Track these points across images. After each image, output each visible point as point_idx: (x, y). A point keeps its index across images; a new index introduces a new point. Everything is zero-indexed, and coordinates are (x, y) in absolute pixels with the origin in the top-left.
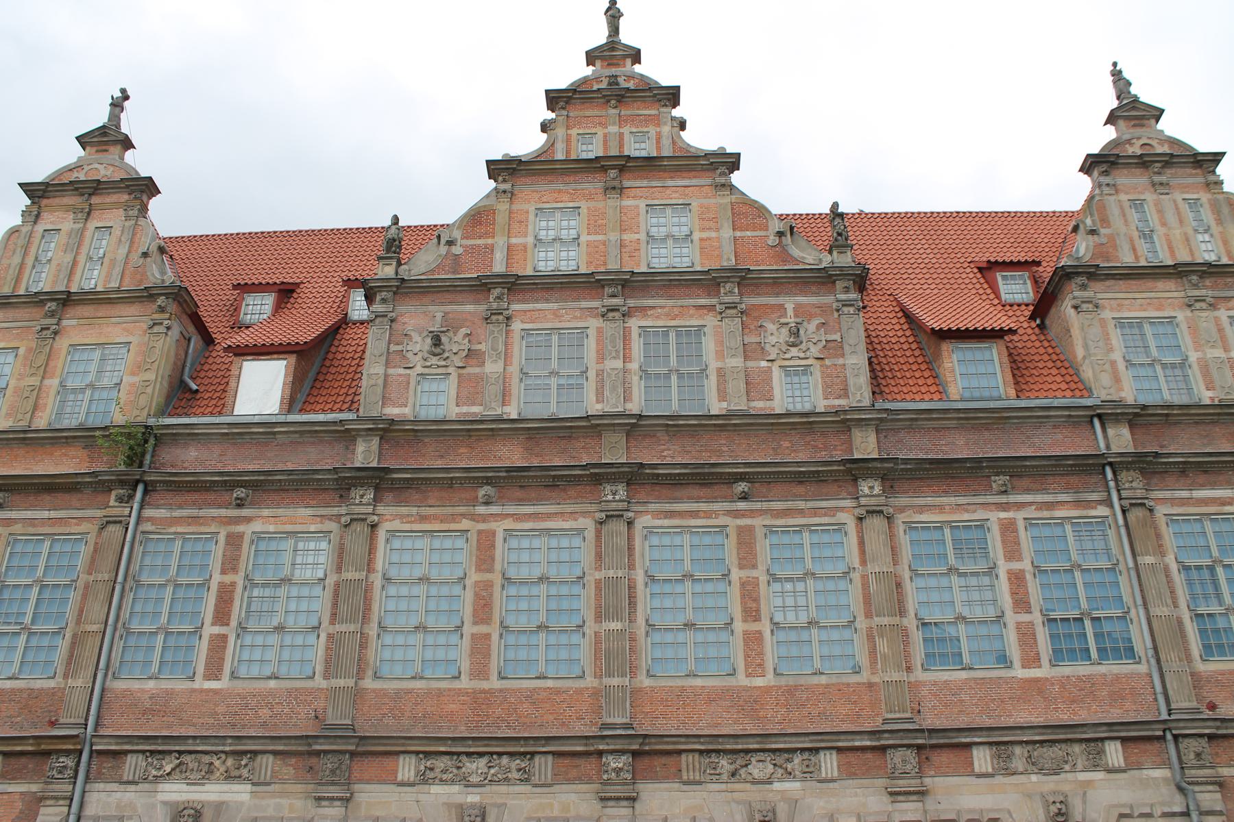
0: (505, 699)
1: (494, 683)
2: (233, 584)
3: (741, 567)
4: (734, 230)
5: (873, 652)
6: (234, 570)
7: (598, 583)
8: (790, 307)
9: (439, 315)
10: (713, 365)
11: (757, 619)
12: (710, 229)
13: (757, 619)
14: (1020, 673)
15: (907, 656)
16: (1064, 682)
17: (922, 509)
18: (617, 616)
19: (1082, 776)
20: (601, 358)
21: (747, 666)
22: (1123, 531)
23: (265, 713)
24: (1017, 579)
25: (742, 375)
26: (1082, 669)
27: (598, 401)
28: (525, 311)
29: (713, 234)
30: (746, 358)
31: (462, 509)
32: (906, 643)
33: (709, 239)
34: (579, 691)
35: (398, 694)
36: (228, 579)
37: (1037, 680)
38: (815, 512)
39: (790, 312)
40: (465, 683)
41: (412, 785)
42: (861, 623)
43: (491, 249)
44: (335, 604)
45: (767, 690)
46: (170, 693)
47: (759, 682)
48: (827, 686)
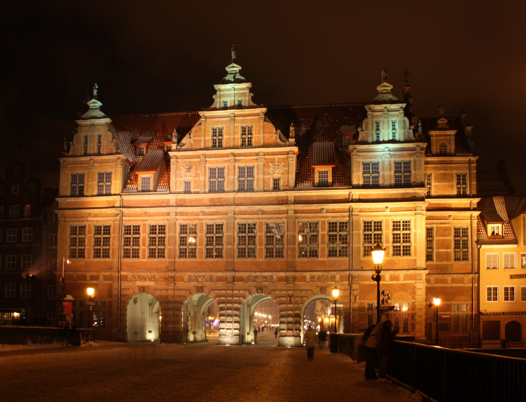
0: (206, 264)
1: (204, 260)
2: (145, 236)
3: (259, 232)
4: (264, 133)
5: (287, 253)
6: (145, 232)
7: (227, 236)
8: (276, 159)
9: (188, 163)
10: (256, 177)
11: (262, 245)
12: (257, 133)
13: (262, 245)
14: (320, 259)
15: (295, 255)
16: (330, 262)
17: (303, 218)
18: (231, 244)
19: (330, 283)
20: (228, 175)
21: (259, 256)
22: (351, 224)
23: (156, 266)
24: (323, 236)
25: (262, 179)
26: (334, 259)
27: (228, 187)
28: (209, 161)
29: (258, 135)
30: (264, 174)
31: (196, 217)
32: (295, 252)
33: (257, 137)
34: (222, 262)
35: (184, 262)
36: (144, 235)
37: (323, 261)
38: (277, 218)
39: (276, 161)
40: (197, 260)
41: (187, 282)
42: (285, 246)
43: (200, 141)
44: (169, 241)
45: (263, 262)
46: (135, 262)
47: (261, 260)
48: (276, 261)
